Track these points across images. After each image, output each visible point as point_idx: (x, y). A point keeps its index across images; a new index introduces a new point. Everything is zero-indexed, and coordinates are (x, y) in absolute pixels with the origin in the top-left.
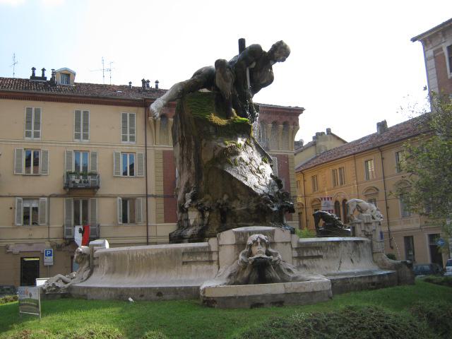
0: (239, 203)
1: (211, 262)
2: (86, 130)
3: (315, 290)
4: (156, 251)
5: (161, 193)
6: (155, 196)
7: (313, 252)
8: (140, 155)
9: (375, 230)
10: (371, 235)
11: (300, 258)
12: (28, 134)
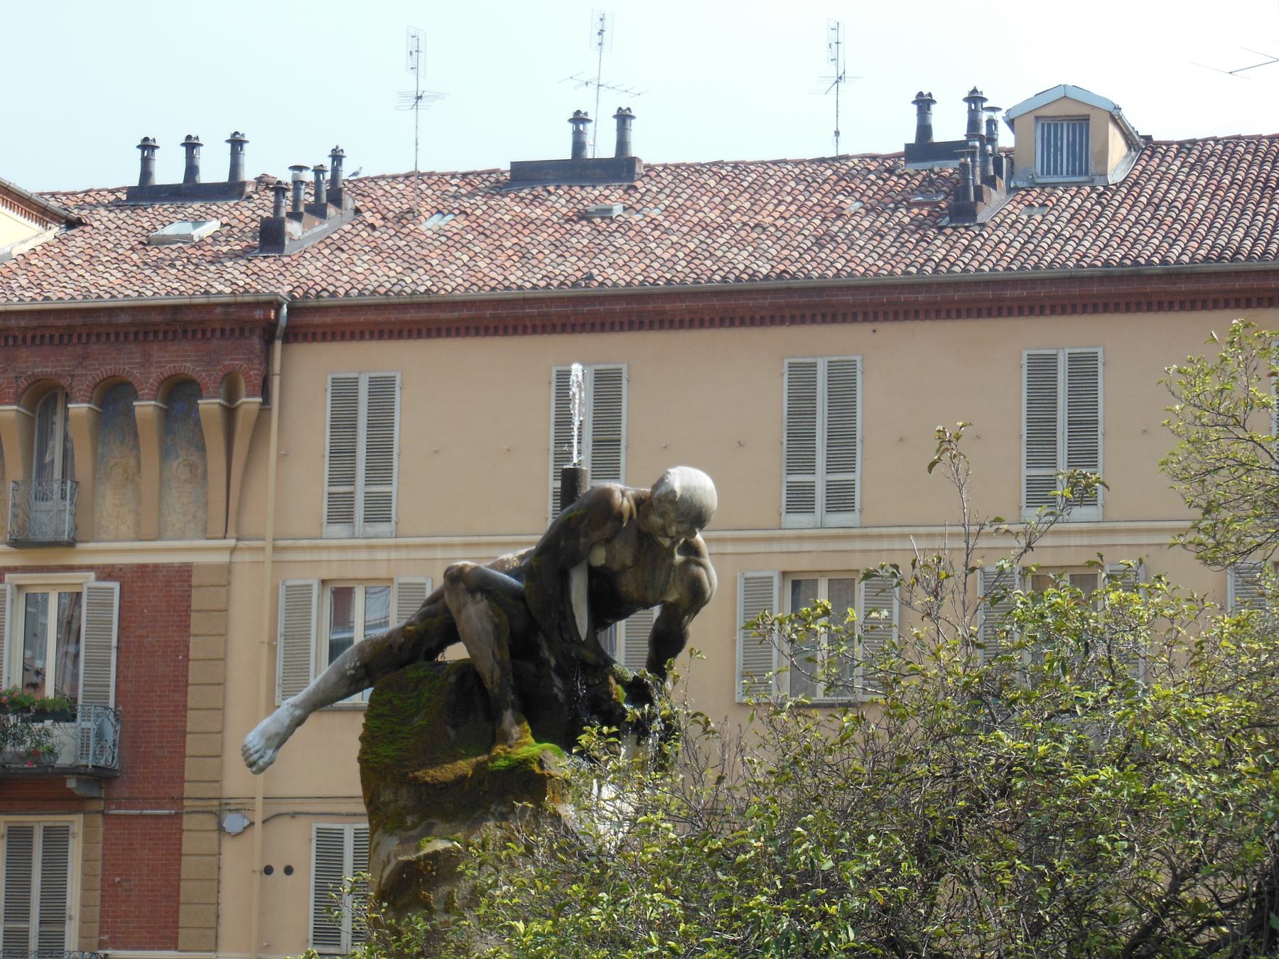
2: (1084, 454)
12: (800, 499)
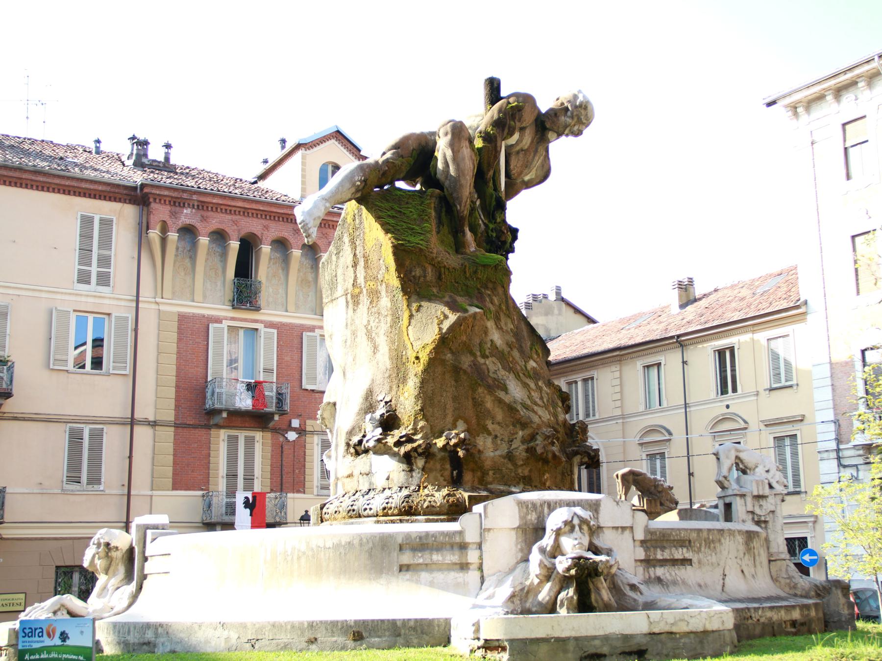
0: (489, 440)
1: (464, 567)
3: (709, 628)
4: (336, 541)
6: (154, 424)
7: (673, 550)
8: (122, 320)
9: (773, 512)
10: (766, 522)
11: (648, 562)
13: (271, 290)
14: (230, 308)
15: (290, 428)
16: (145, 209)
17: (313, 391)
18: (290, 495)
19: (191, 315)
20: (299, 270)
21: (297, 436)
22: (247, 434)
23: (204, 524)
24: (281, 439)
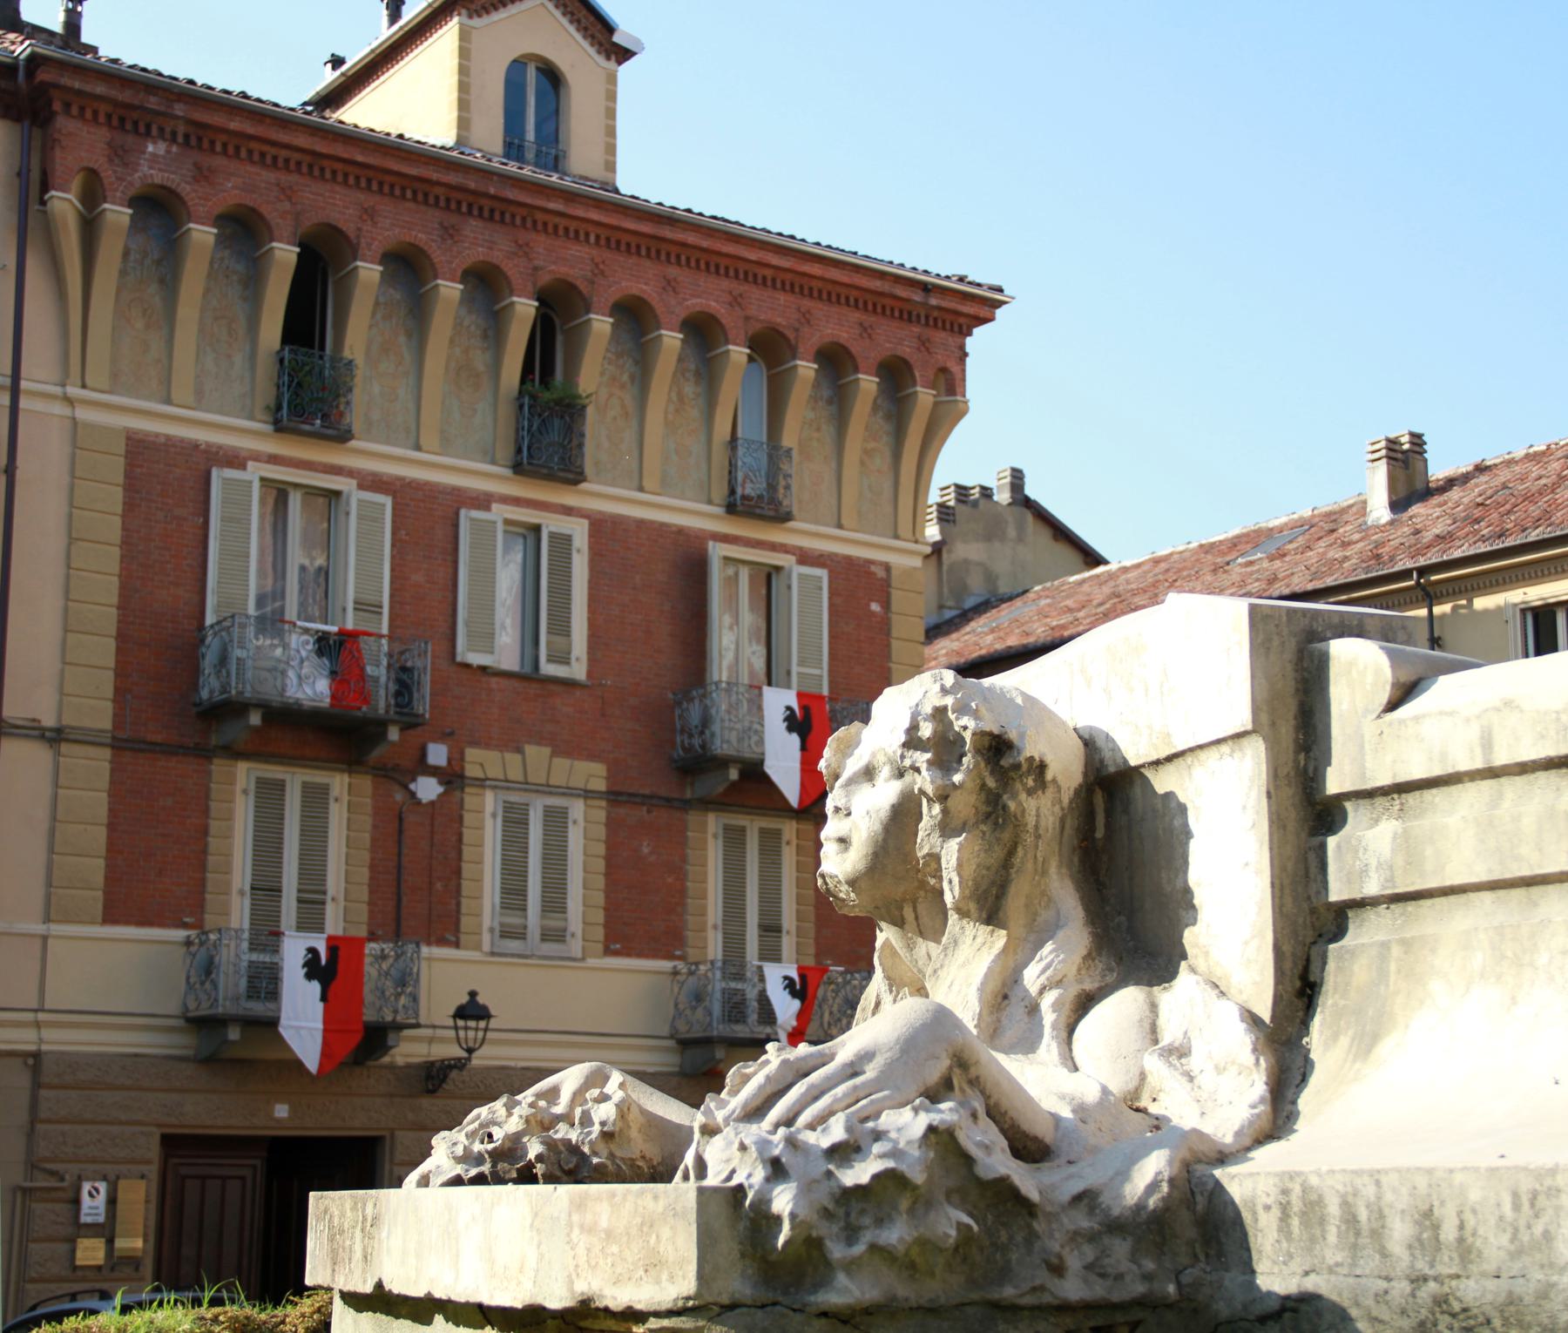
5: (100, 716)
6: (55, 737)
13: (376, 389)
14: (269, 428)
15: (422, 767)
16: (37, 133)
17: (483, 669)
18: (425, 950)
19: (163, 440)
20: (452, 341)
21: (440, 789)
22: (308, 778)
23: (189, 1020)
24: (399, 796)
